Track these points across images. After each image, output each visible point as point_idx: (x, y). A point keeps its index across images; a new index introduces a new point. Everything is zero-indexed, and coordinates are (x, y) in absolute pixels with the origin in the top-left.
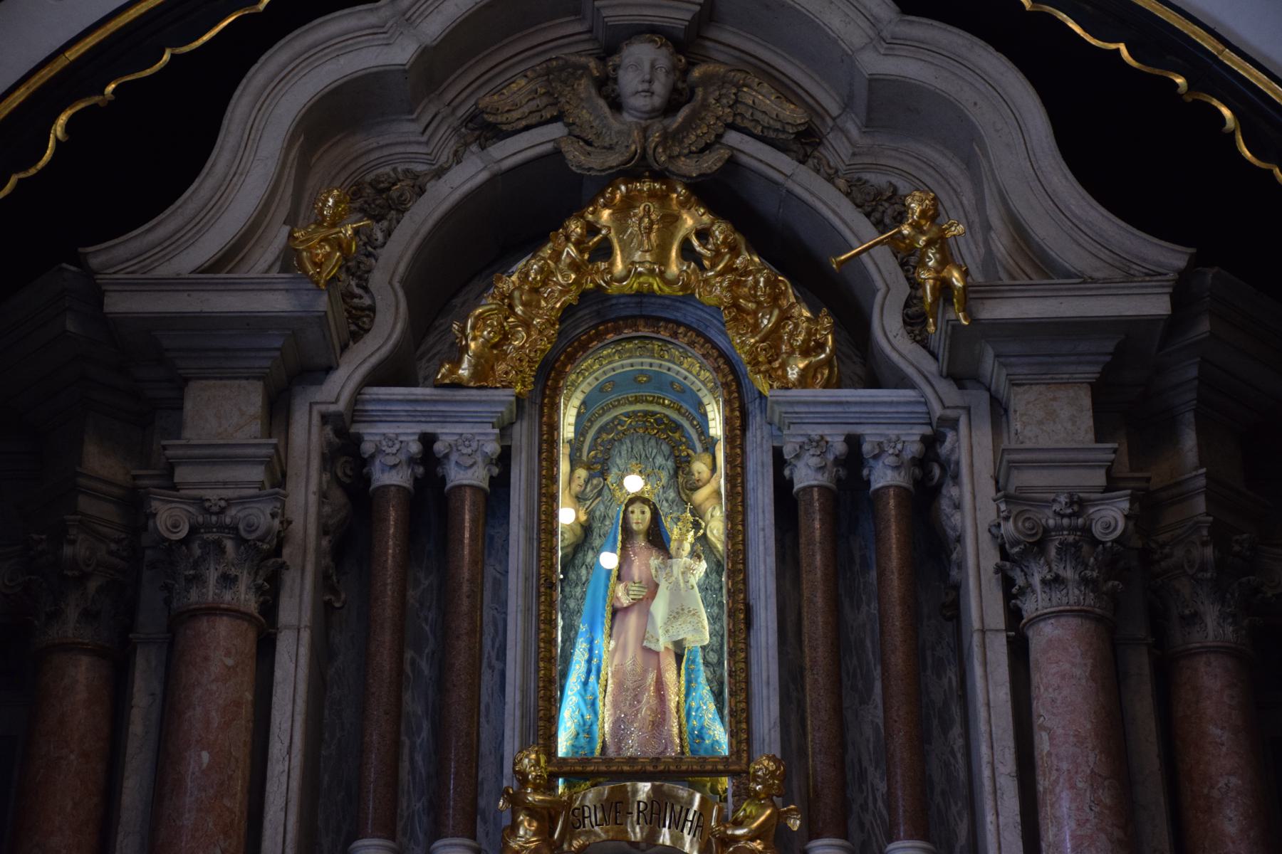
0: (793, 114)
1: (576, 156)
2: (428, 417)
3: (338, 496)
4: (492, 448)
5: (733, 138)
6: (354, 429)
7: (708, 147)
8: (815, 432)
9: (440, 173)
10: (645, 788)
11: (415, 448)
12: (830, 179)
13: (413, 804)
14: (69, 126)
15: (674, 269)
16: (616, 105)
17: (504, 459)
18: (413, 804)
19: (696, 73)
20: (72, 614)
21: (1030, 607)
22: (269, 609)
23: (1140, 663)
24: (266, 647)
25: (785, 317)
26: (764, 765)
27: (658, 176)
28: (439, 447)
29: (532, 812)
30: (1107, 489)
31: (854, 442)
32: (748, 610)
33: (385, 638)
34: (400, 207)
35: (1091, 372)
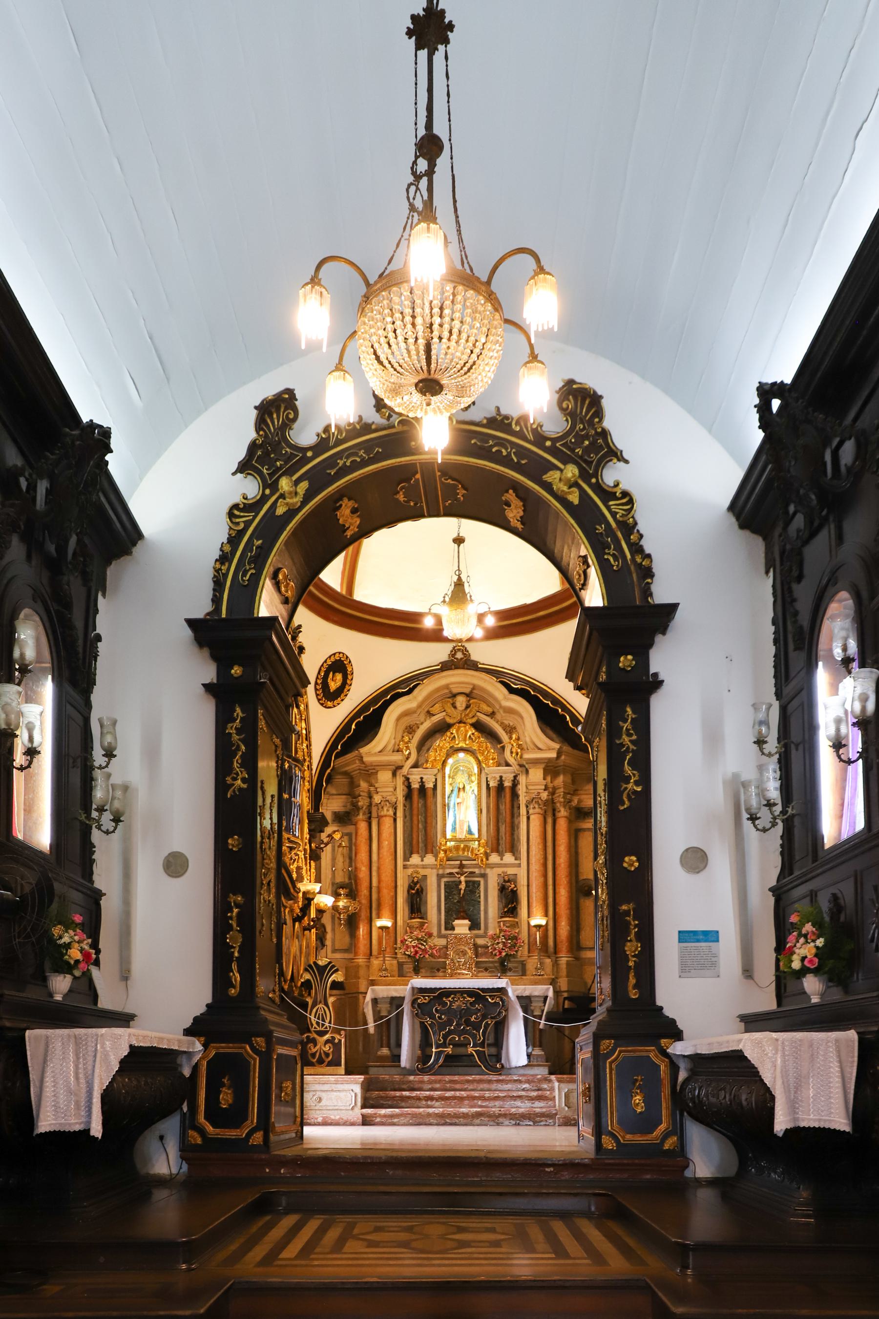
0: (490, 710)
1: (448, 720)
2: (421, 774)
3: (406, 789)
4: (434, 780)
5: (478, 714)
6: (408, 776)
7: (473, 717)
8: (494, 775)
9: (422, 723)
10: (462, 846)
11: (419, 780)
12: (497, 722)
13: (421, 845)
14: (356, 725)
15: (467, 742)
16: (455, 707)
17: (436, 779)
18: (421, 845)
19: (471, 701)
20: (361, 814)
21: (531, 811)
22: (395, 814)
23: (550, 821)
24: (395, 820)
25: (488, 752)
26: (483, 841)
27: (464, 723)
28: (424, 780)
29: (443, 850)
30: (545, 790)
31: (501, 777)
32: (481, 810)
33: (415, 818)
34: (414, 731)
35: (543, 766)
